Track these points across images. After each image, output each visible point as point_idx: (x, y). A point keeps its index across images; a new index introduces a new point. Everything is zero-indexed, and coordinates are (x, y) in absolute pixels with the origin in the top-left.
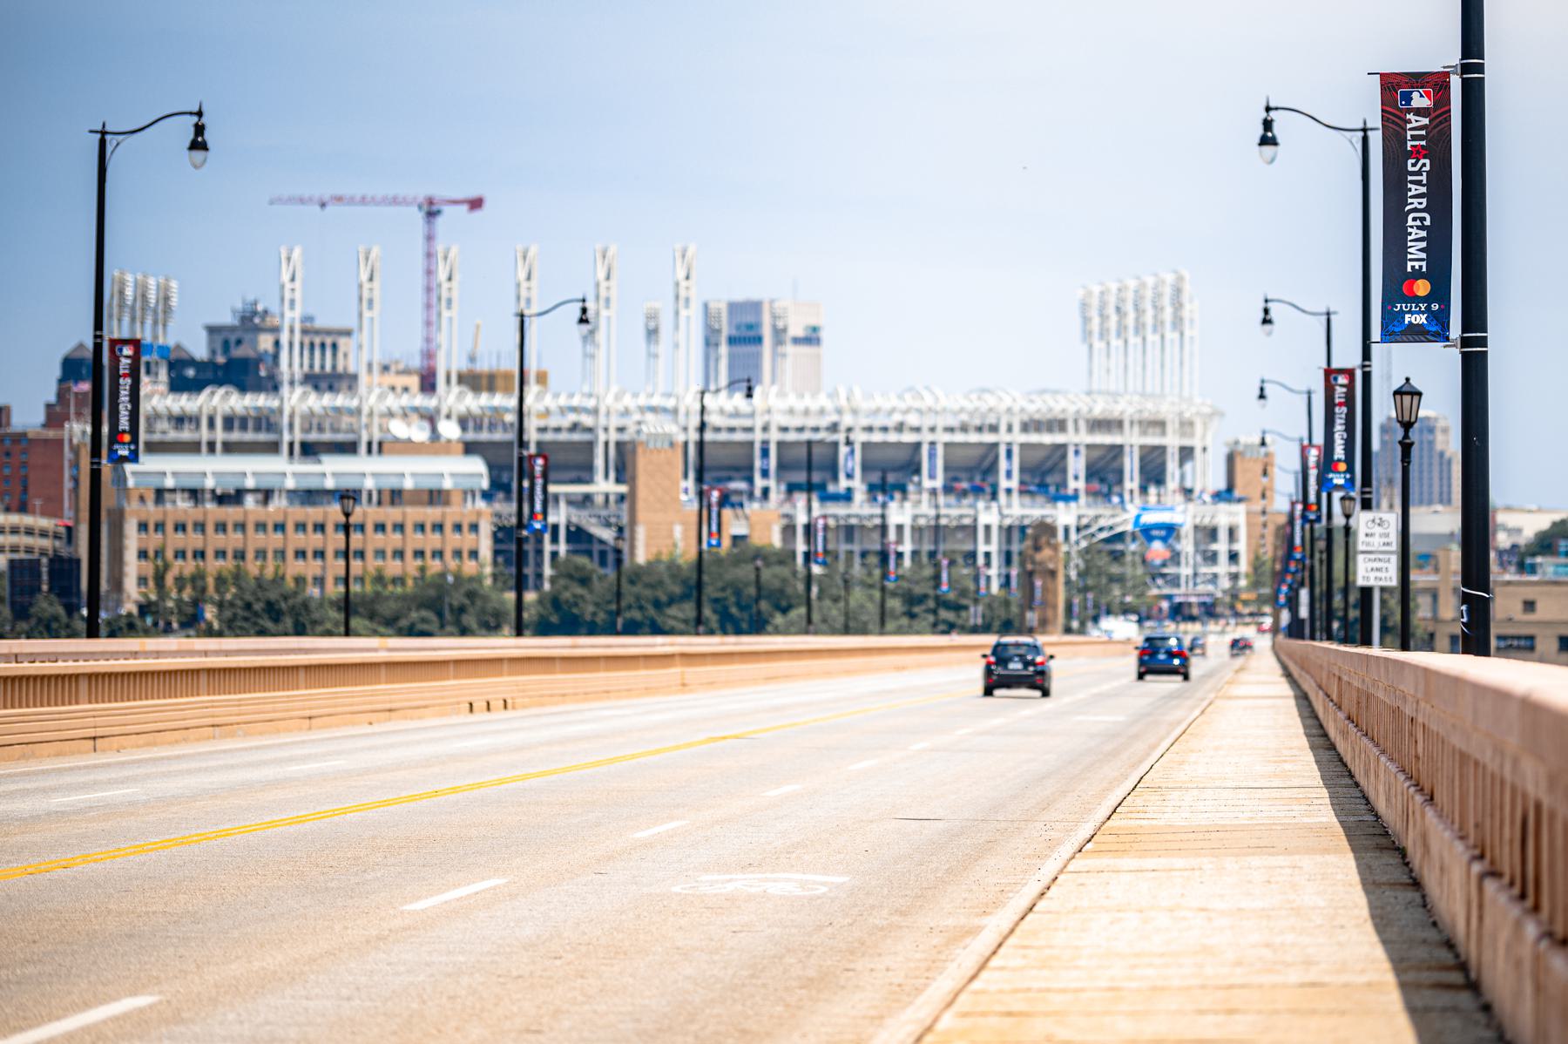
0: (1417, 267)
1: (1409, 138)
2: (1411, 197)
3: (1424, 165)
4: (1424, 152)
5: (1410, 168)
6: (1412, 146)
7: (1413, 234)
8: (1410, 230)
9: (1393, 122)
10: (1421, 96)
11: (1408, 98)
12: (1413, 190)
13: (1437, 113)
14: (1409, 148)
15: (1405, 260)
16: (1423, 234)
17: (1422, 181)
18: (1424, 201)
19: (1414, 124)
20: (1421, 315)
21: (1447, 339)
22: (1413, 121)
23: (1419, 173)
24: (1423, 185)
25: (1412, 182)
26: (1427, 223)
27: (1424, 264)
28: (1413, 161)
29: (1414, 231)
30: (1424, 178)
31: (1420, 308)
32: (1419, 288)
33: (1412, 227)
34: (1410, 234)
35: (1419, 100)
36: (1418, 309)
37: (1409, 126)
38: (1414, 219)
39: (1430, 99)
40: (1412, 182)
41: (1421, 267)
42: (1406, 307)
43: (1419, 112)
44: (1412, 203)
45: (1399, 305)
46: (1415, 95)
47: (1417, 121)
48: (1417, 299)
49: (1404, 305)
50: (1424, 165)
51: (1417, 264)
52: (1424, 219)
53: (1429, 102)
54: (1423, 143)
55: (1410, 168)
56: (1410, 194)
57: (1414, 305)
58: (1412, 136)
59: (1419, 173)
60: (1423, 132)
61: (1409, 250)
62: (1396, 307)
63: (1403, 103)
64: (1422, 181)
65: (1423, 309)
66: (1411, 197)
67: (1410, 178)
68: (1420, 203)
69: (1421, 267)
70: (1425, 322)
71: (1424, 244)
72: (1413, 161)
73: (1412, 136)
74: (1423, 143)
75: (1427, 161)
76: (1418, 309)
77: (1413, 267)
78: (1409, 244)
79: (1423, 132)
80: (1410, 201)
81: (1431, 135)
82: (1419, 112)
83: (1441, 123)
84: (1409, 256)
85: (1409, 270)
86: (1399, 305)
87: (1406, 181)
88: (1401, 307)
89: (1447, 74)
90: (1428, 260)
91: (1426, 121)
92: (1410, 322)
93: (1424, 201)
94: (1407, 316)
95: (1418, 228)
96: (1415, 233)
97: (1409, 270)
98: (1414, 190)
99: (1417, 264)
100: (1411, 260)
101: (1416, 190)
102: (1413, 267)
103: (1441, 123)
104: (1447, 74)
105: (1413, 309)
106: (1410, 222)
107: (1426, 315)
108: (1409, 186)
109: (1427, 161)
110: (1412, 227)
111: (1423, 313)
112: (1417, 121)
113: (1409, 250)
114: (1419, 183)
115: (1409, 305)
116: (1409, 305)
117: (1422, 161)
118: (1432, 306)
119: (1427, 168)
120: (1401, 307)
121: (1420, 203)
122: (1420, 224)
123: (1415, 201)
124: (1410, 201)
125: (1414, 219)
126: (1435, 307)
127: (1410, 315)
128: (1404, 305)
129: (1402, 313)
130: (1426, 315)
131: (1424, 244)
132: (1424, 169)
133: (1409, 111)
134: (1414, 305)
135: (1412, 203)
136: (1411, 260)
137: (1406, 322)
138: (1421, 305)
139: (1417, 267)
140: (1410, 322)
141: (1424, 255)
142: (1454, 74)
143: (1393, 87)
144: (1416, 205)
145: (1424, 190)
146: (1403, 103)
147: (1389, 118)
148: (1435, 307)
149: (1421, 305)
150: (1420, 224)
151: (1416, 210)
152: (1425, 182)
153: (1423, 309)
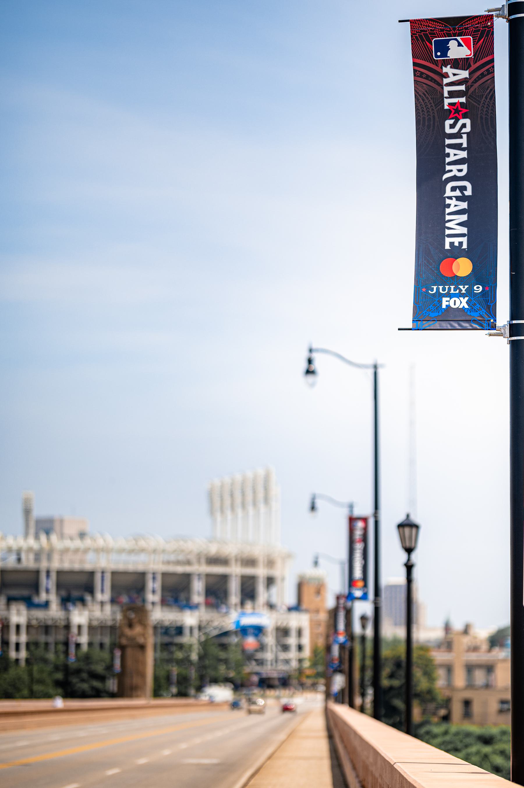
0: (456, 244)
1: (446, 94)
2: (450, 164)
3: (464, 126)
4: (464, 111)
5: (448, 130)
6: (450, 104)
7: (452, 206)
8: (448, 201)
9: (428, 77)
10: (460, 45)
11: (444, 48)
12: (452, 155)
13: (478, 64)
14: (446, 107)
15: (443, 236)
16: (464, 205)
17: (462, 144)
18: (465, 167)
19: (452, 79)
20: (461, 299)
21: (494, 327)
22: (450, 75)
23: (458, 135)
24: (463, 149)
25: (451, 146)
26: (468, 192)
27: (464, 240)
28: (452, 122)
29: (453, 202)
30: (464, 141)
31: (461, 290)
32: (458, 269)
33: (450, 198)
34: (449, 206)
36: (457, 292)
37: (446, 81)
38: (453, 189)
39: (469, 48)
40: (451, 146)
41: (461, 243)
42: (444, 290)
43: (457, 64)
44: (451, 171)
45: (435, 287)
46: (453, 44)
47: (454, 75)
48: (457, 280)
49: (441, 287)
50: (464, 126)
53: (469, 52)
54: (463, 100)
55: (448, 130)
56: (448, 160)
57: (452, 287)
58: (449, 92)
59: (458, 135)
60: (463, 88)
61: (447, 225)
62: (432, 290)
63: (439, 54)
64: (462, 144)
65: (464, 292)
66: (450, 164)
67: (448, 142)
68: (460, 171)
69: (461, 243)
70: (466, 306)
71: (464, 218)
72: (452, 122)
73: (449, 92)
74: (463, 100)
75: (468, 121)
76: (457, 292)
77: (452, 244)
78: (448, 218)
79: (463, 88)
80: (448, 168)
81: (472, 89)
82: (457, 64)
83: (483, 75)
84: (448, 232)
85: (447, 247)
86: (435, 287)
87: (444, 146)
88: (438, 289)
89: (490, 18)
90: (469, 235)
91: (464, 74)
92: (448, 306)
93: (465, 167)
94: (444, 299)
95: (458, 198)
96: (454, 205)
97: (447, 247)
98: (454, 155)
99: (456, 241)
100: (450, 236)
101: (455, 155)
102: (452, 244)
103: (483, 75)
104: (490, 18)
105: (452, 292)
106: (448, 193)
107: (467, 299)
108: (448, 150)
109: (468, 121)
110: (450, 198)
111: (464, 296)
112: (454, 75)
113: (447, 225)
114: (458, 147)
115: (447, 287)
116: (447, 287)
117: (461, 122)
118: (475, 288)
119: (468, 129)
120: (438, 289)
121: (460, 171)
122: (460, 194)
123: (454, 168)
124: (448, 168)
125: (453, 189)
127: (448, 299)
128: (441, 287)
129: (439, 296)
130: (467, 299)
131: (464, 218)
132: (464, 130)
133: (445, 63)
134: (452, 287)
135: (451, 171)
136: (450, 236)
137: (444, 306)
138: (461, 287)
139: (456, 244)
140: (448, 306)
141: (464, 230)
142: (498, 16)
143: (426, 35)
144: (455, 173)
145: (463, 154)
146: (439, 54)
147: (422, 73)
149: (461, 287)
150: (460, 194)
151: (455, 178)
152: (465, 145)
153: (464, 292)
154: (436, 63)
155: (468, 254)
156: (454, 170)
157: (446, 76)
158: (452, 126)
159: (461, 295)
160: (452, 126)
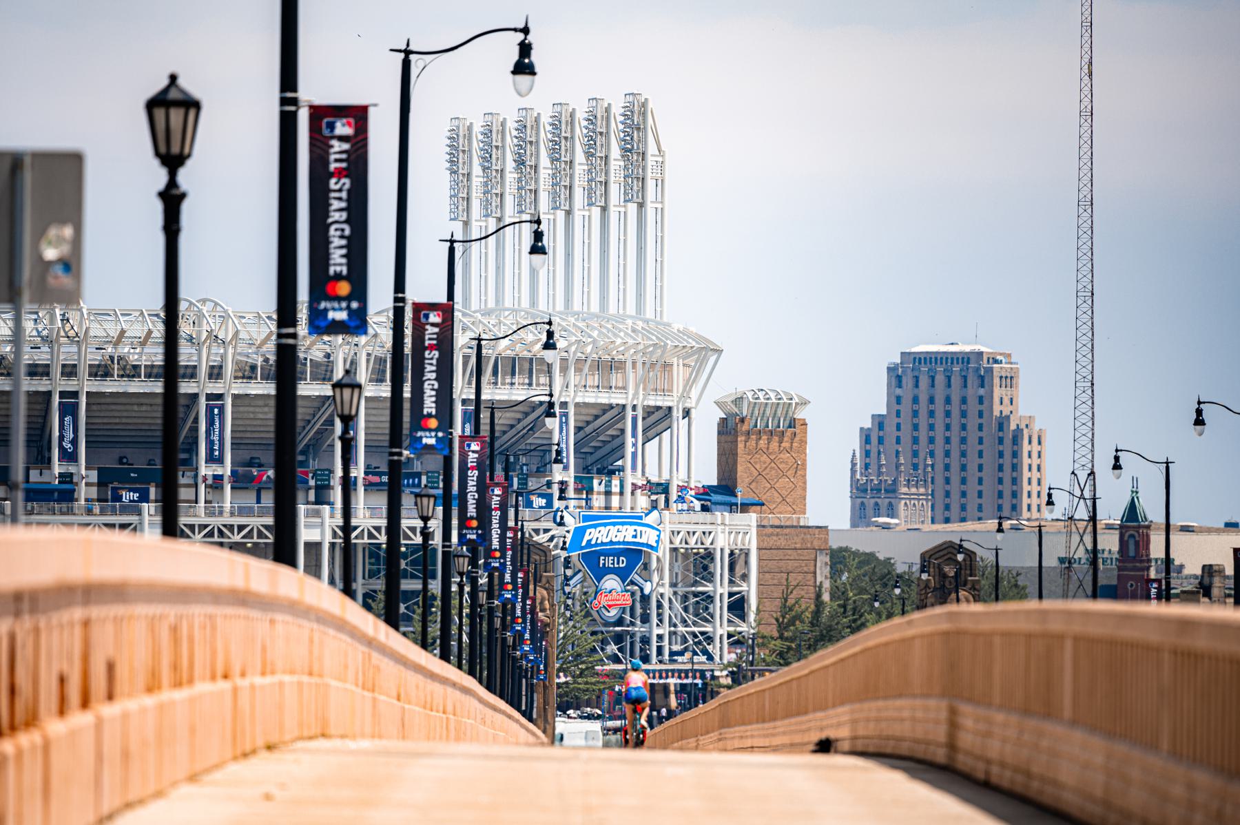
3: (344, 184)
4: (344, 173)
15: (327, 265)
19: (336, 149)
26: (347, 232)
33: (334, 236)
35: (342, 128)
38: (336, 230)
43: (342, 139)
50: (344, 184)
51: (338, 269)
52: (343, 230)
59: (340, 190)
77: (335, 271)
82: (342, 139)
90: (349, 265)
96: (336, 242)
98: (336, 205)
102: (335, 271)
124: (332, 214)
125: (336, 230)
126: (355, 305)
131: (344, 251)
133: (333, 137)
136: (335, 265)
141: (344, 261)
148: (355, 305)
154: (326, 137)
155: (347, 278)
156: (336, 216)
157: (332, 146)
158: (336, 183)
159: (341, 309)
160: (336, 183)
